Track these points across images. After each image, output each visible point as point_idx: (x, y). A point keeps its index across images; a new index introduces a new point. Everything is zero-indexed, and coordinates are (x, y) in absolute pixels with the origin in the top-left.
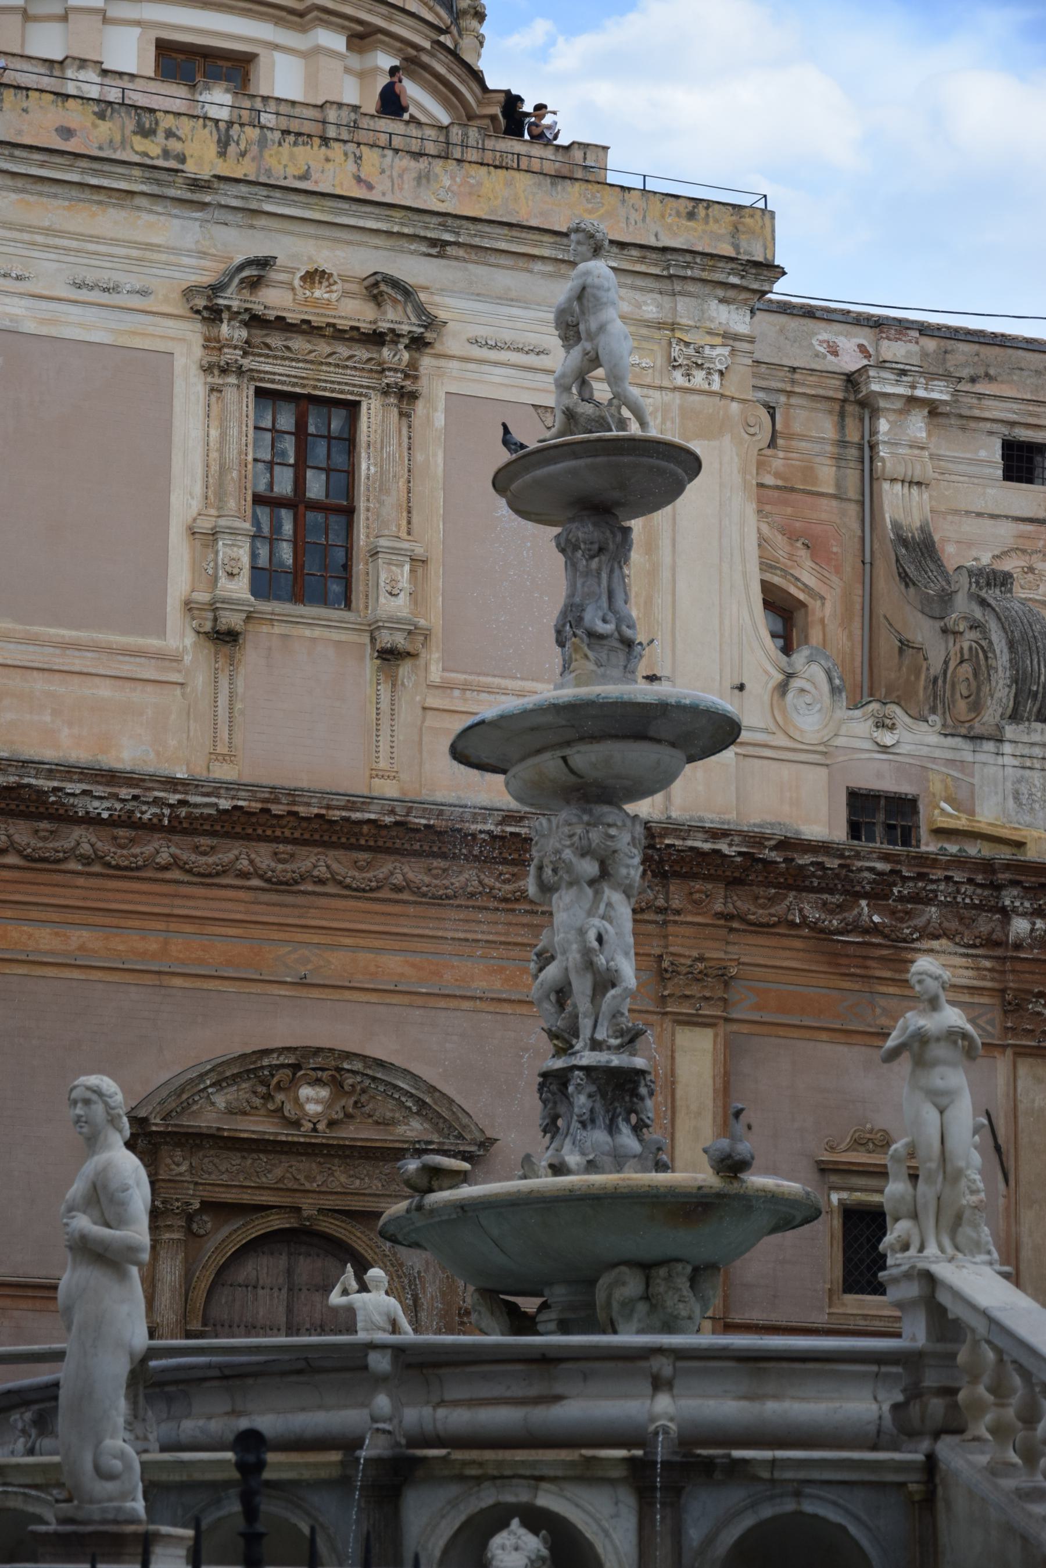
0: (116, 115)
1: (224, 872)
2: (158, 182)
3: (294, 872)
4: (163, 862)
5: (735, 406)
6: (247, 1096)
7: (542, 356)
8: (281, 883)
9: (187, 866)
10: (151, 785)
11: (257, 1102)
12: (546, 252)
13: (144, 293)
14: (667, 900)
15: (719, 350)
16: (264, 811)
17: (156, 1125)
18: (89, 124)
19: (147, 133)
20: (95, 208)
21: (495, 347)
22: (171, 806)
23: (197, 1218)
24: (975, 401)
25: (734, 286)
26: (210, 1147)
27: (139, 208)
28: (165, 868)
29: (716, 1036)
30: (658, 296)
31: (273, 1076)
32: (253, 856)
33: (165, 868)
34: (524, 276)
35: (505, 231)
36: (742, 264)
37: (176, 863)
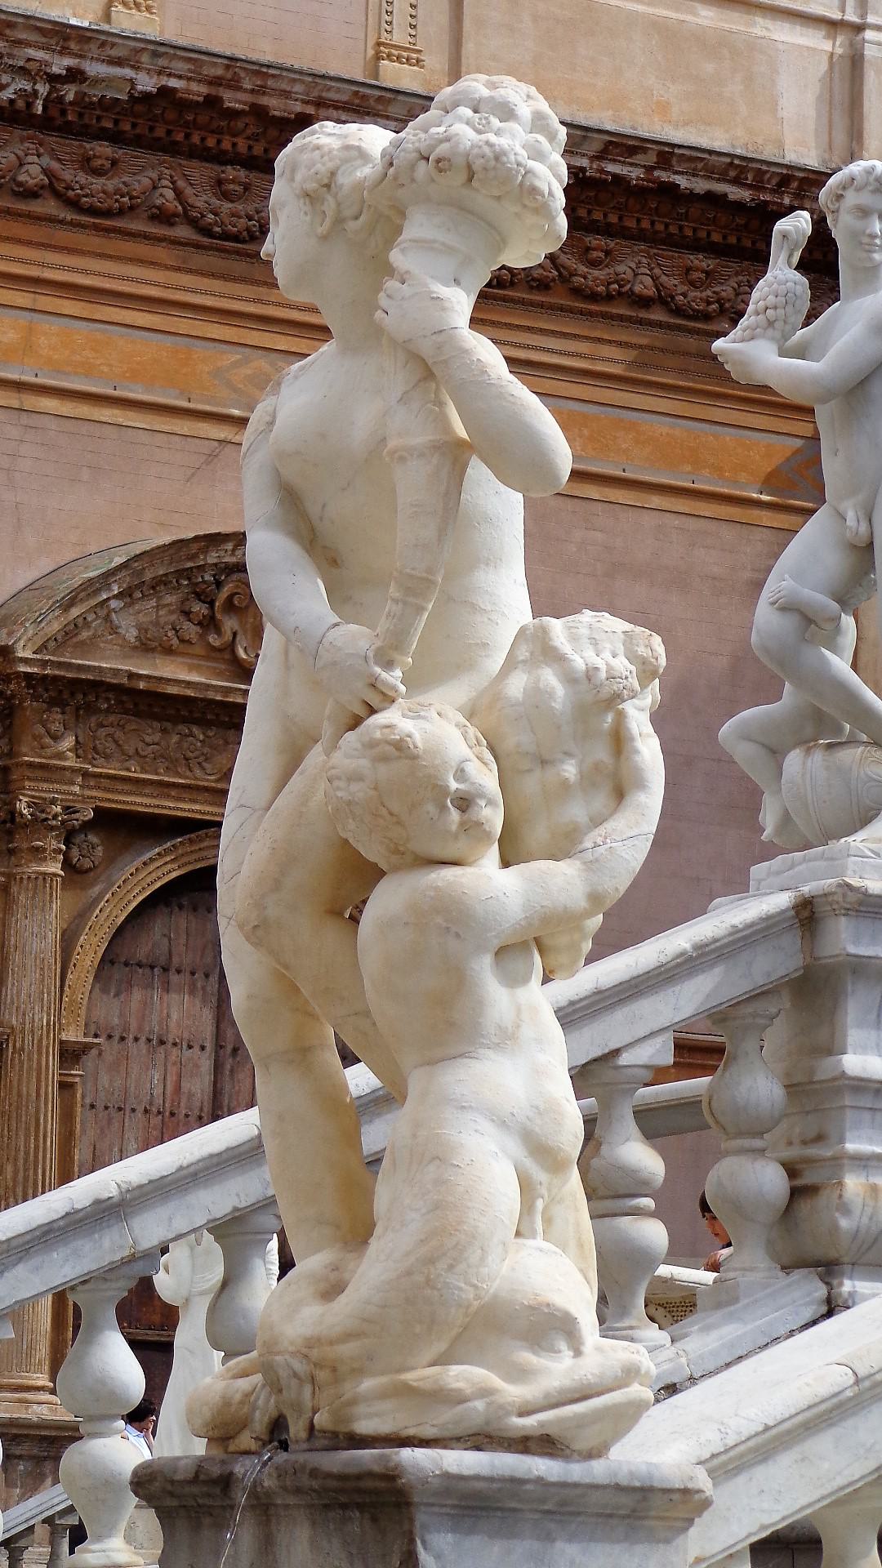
1: (132, 208)
3: (250, 218)
4: (31, 182)
6: (173, 617)
8: (226, 236)
9: (71, 193)
10: (23, 36)
11: (191, 630)
16: (212, 102)
17: (26, 661)
22: (53, 79)
23: (79, 839)
26: (108, 711)
28: (31, 194)
31: (219, 584)
32: (181, 183)
33: (31, 194)
37: (53, 188)
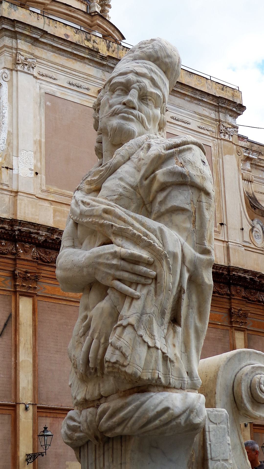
0: (80, 33)
2: (92, 55)
5: (235, 146)
7: (189, 125)
12: (190, 94)
13: (88, 89)
14: (230, 291)
15: (231, 129)
18: (73, 35)
19: (89, 40)
20: (74, 61)
21: (178, 120)
24: (259, 161)
25: (234, 111)
27: (86, 63)
29: (245, 334)
30: (215, 112)
34: (183, 100)
35: (180, 86)
36: (237, 105)
